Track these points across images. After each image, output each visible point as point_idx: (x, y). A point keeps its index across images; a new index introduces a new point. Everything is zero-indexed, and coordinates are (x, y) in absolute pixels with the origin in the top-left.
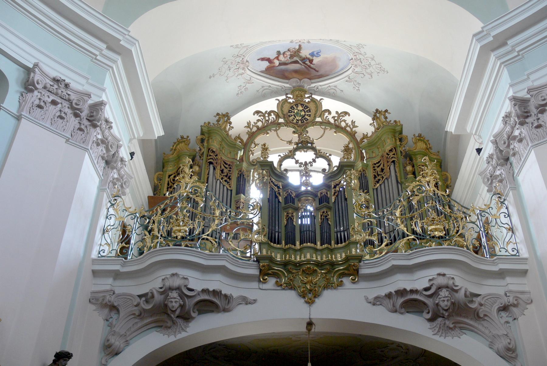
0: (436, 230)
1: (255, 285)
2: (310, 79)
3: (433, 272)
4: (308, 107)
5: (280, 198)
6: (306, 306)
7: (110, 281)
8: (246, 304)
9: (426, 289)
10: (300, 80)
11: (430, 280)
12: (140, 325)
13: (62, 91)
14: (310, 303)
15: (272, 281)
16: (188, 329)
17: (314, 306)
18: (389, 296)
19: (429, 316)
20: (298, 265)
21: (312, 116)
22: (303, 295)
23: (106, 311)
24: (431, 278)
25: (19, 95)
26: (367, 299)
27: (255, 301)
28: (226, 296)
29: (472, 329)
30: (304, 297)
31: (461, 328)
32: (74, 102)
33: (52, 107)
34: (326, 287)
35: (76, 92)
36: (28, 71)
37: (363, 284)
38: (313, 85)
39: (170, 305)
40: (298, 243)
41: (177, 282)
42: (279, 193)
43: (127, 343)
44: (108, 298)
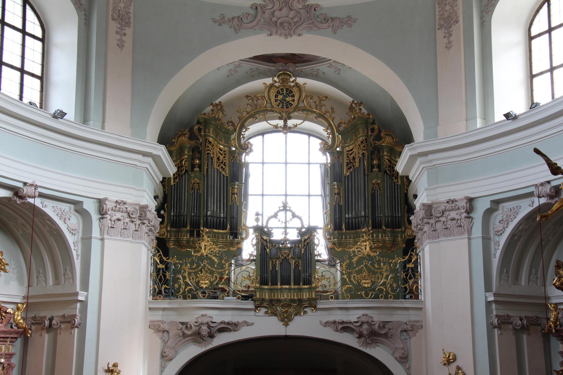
0: (365, 283)
1: (252, 313)
2: (295, 63)
3: (360, 313)
4: (292, 92)
5: (268, 250)
6: (284, 327)
7: (161, 312)
8: (247, 326)
9: (355, 322)
10: (286, 64)
11: (358, 318)
12: (183, 341)
13: (123, 207)
14: (286, 325)
15: (264, 310)
16: (213, 343)
17: (289, 326)
18: (335, 322)
19: (357, 336)
20: (279, 301)
21: (296, 101)
22: (282, 320)
23: (161, 334)
24: (358, 316)
25: (98, 221)
26: (321, 322)
27: (253, 324)
28: (235, 324)
29: (383, 343)
30: (282, 321)
31: (376, 343)
32: (131, 213)
33: (118, 222)
34: (296, 315)
35: (131, 204)
36: (101, 202)
37: (319, 313)
38: (298, 68)
39: (203, 333)
40: (279, 284)
41: (205, 320)
42: (267, 246)
43: (176, 353)
44: (162, 325)
